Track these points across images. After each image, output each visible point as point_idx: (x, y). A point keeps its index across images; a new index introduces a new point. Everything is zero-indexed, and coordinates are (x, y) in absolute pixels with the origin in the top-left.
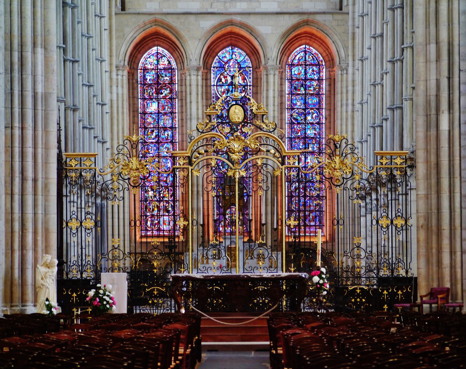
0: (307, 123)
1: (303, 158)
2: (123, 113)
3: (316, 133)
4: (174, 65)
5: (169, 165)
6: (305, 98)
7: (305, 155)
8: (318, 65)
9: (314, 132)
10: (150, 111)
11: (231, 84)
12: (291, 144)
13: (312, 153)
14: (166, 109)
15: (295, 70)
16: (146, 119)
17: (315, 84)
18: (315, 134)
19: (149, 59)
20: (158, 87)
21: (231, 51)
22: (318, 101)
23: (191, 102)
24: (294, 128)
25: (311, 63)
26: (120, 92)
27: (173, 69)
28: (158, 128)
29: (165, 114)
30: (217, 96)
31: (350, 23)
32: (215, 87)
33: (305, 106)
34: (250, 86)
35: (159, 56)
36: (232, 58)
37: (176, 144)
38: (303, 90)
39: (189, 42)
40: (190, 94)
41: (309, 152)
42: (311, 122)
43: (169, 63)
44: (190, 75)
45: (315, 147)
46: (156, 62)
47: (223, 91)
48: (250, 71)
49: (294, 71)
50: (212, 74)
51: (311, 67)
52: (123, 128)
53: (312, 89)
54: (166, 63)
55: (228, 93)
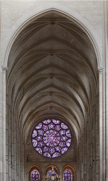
4: (39, 174)
8: (71, 174)
15: (65, 175)
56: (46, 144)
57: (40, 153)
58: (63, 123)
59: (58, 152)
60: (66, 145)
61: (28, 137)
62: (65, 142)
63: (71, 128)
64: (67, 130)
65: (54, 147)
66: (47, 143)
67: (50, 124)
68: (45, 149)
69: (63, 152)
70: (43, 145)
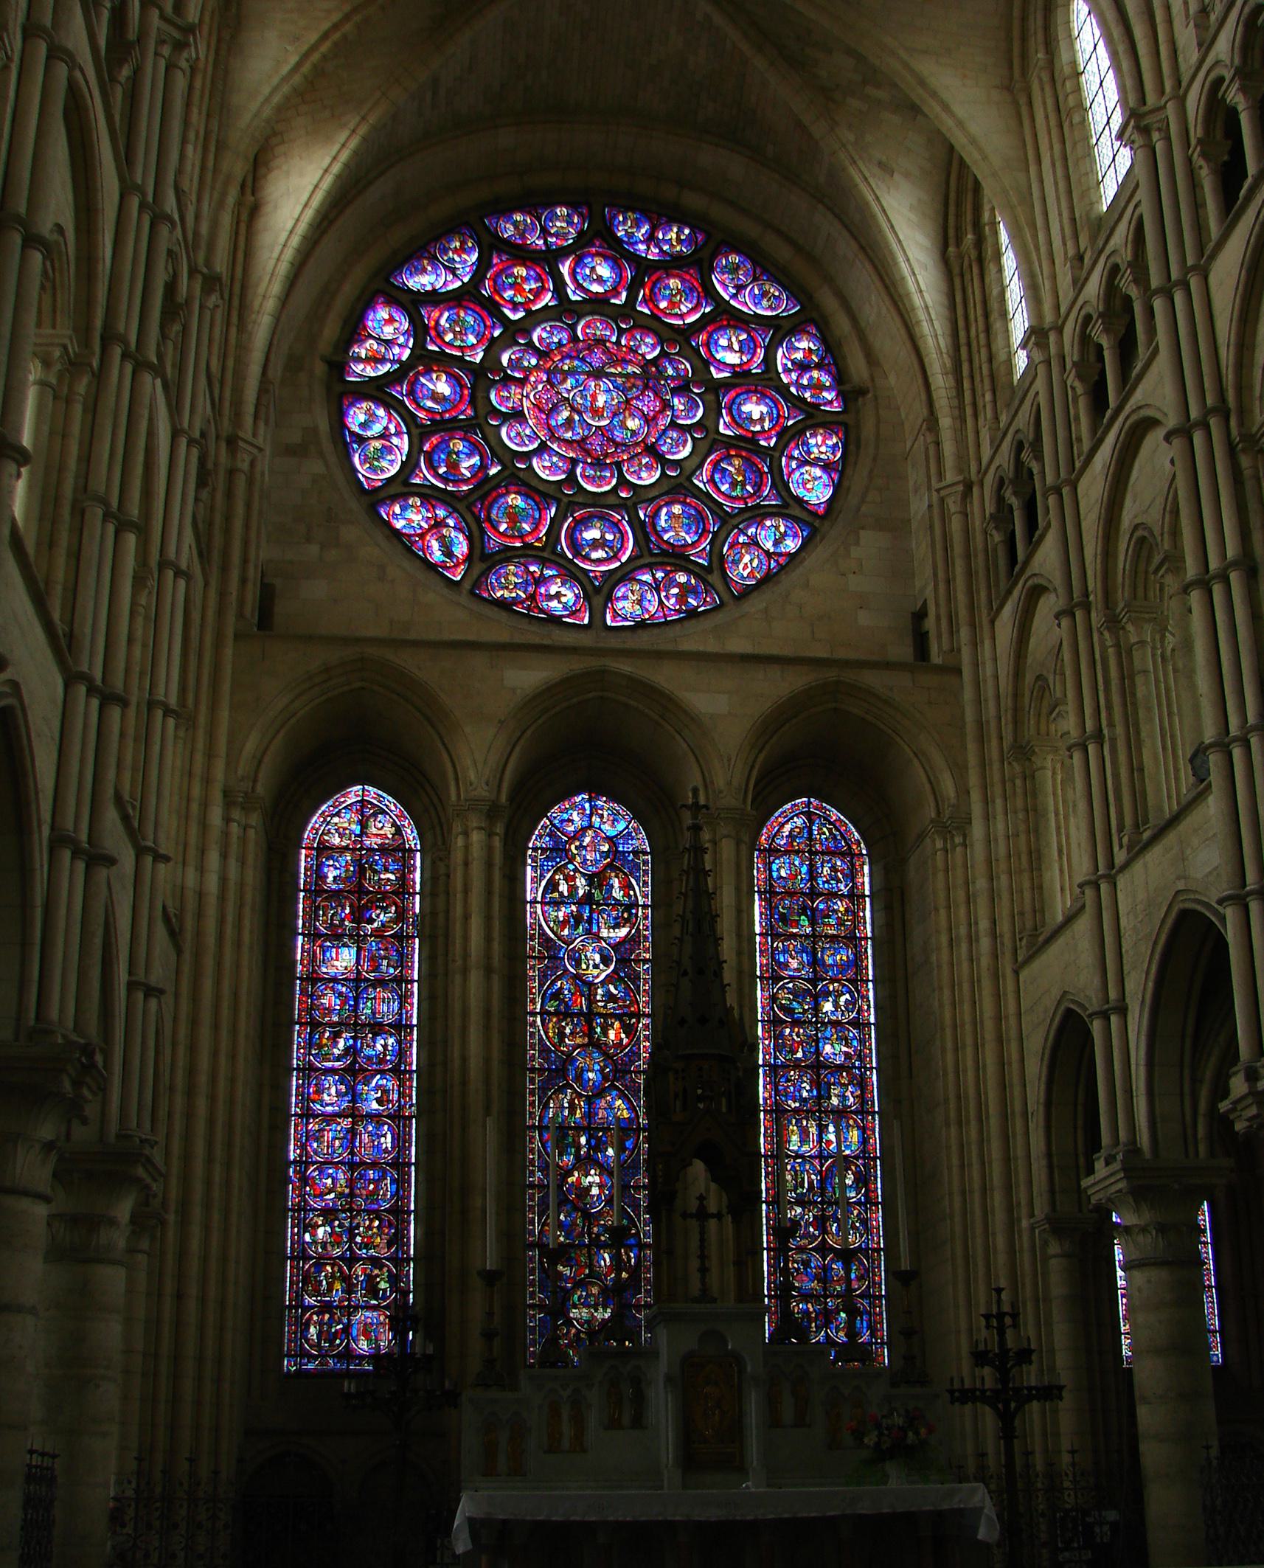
0: (823, 1023)
1: (813, 1130)
2: (238, 944)
3: (851, 1051)
5: (387, 1142)
6: (814, 949)
7: (820, 1119)
8: (849, 855)
9: (844, 1049)
10: (332, 971)
11: (588, 898)
12: (776, 1085)
13: (841, 1114)
14: (384, 968)
15: (781, 869)
16: (319, 998)
17: (842, 909)
18: (846, 1054)
19: (336, 820)
20: (360, 900)
21: (587, 806)
22: (851, 957)
23: (467, 917)
24: (782, 1035)
25: (827, 847)
26: (233, 873)
27: (410, 850)
28: (356, 1024)
29: (380, 982)
30: (545, 933)
31: (968, 694)
32: (539, 906)
33: (815, 972)
34: (645, 906)
35: (365, 812)
36: (591, 826)
37: (411, 1079)
38: (807, 923)
39: (468, 730)
40: (466, 891)
41: (832, 1111)
42: (834, 1018)
43: (398, 831)
44: (466, 834)
45: (848, 1094)
46: (357, 829)
47: (561, 919)
48: (645, 863)
49: (778, 870)
50: (529, 868)
51: (827, 858)
52: (236, 995)
53: (832, 921)
54: (389, 831)
55: (576, 927)
56: (527, 456)
57: (437, 555)
58: (738, 253)
59: (676, 557)
60: (781, 485)
61: (295, 365)
62: (772, 455)
63: (829, 302)
64: (781, 330)
65: (629, 508)
66: (543, 449)
67: (579, 250)
68: (514, 517)
69: (746, 567)
70: (483, 467)
